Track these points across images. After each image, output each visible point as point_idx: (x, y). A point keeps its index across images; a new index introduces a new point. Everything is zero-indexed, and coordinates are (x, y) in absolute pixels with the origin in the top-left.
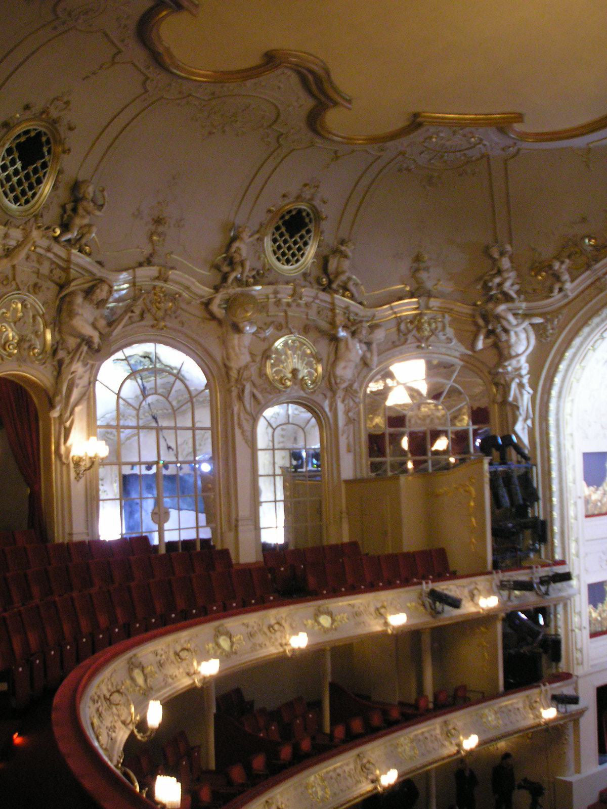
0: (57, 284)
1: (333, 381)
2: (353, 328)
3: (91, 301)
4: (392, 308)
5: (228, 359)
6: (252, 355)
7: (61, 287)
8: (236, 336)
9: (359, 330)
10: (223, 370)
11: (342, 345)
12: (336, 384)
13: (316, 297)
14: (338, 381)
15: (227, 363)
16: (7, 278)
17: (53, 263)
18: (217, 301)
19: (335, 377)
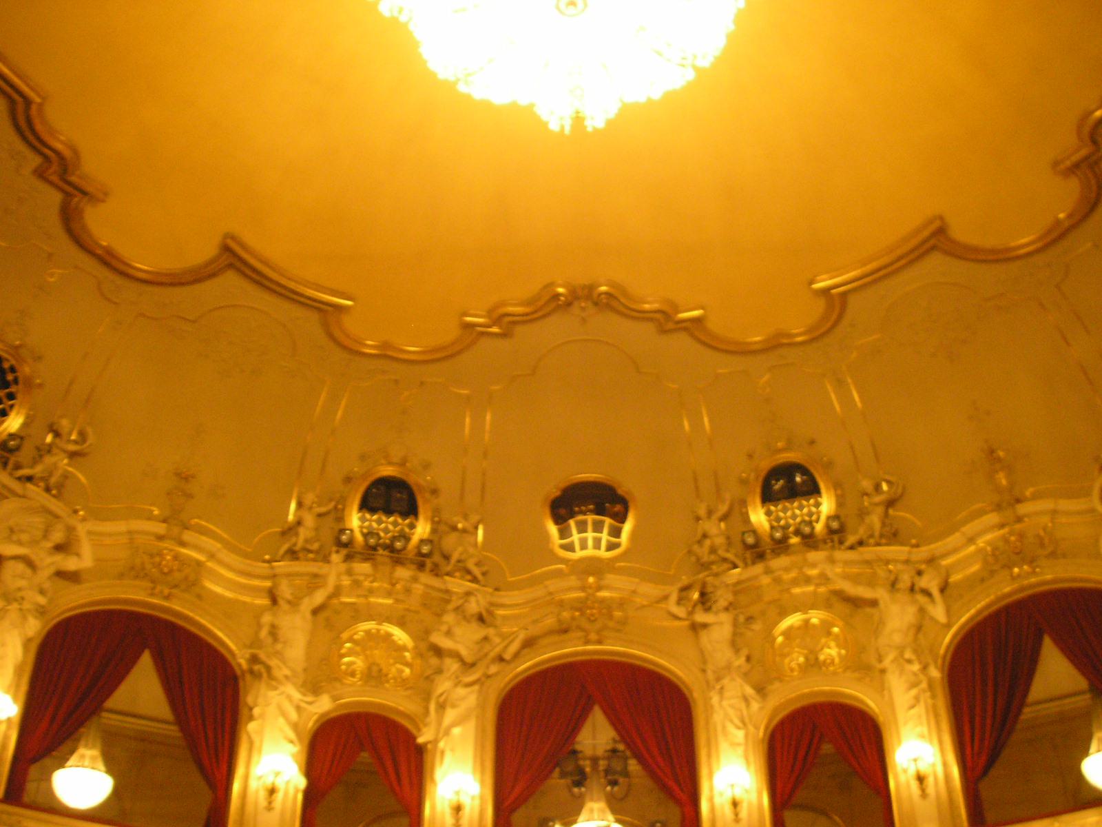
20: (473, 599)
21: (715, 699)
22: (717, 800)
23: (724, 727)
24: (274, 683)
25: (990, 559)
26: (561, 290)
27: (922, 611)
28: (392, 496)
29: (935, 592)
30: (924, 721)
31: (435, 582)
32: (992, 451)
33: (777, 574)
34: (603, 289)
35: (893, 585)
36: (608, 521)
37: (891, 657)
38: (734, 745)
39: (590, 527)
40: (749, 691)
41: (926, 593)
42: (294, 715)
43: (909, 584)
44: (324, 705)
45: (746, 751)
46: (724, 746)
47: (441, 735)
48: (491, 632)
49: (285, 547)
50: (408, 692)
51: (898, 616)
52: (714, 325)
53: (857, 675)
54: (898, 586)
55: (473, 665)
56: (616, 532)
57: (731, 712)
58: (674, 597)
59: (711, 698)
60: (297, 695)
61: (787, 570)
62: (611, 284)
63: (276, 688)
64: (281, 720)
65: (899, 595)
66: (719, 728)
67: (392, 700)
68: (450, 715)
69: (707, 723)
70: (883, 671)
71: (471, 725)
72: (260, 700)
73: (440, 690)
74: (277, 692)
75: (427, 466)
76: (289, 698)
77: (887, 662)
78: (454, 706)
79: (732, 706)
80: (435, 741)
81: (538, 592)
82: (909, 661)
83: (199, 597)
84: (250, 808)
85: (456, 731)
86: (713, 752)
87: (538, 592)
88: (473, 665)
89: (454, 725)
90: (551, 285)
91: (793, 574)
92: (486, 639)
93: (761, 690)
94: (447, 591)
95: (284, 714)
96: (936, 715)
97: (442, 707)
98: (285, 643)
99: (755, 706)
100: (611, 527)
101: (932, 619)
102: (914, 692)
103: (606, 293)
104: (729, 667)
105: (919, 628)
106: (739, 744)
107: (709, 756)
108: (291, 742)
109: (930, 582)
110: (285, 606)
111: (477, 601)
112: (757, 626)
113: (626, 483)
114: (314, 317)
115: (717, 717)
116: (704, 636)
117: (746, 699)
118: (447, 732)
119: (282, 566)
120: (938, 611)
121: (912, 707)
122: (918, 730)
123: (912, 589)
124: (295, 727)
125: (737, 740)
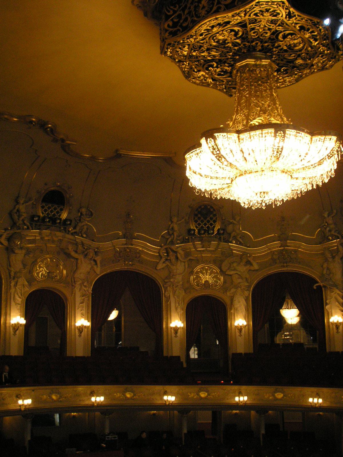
1: (73, 280)
2: (86, 253)
4: (112, 242)
5: (10, 266)
6: (25, 266)
8: (14, 255)
10: (7, 271)
11: (79, 261)
12: (75, 281)
14: (76, 281)
15: (9, 268)
18: (4, 236)
19: (74, 278)
21: (13, 284)
25: (118, 254)
27: (92, 267)
29: (98, 262)
30: (84, 308)
32: (128, 215)
33: (43, 236)
35: (86, 255)
37: (79, 283)
38: (16, 304)
40: (26, 283)
41: (95, 261)
45: (21, 307)
46: (13, 303)
51: (84, 267)
53: (64, 285)
58: (4, 236)
59: (10, 283)
61: (47, 236)
69: (7, 292)
82: (85, 286)
91: (49, 238)
93: (30, 284)
96: (88, 306)
99: (27, 289)
101: (95, 272)
102: (83, 298)
105: (89, 273)
109: (98, 259)
112: (31, 256)
115: (13, 290)
116: (13, 257)
120: (98, 270)
121: (81, 303)
123: (91, 259)
125: (18, 302)
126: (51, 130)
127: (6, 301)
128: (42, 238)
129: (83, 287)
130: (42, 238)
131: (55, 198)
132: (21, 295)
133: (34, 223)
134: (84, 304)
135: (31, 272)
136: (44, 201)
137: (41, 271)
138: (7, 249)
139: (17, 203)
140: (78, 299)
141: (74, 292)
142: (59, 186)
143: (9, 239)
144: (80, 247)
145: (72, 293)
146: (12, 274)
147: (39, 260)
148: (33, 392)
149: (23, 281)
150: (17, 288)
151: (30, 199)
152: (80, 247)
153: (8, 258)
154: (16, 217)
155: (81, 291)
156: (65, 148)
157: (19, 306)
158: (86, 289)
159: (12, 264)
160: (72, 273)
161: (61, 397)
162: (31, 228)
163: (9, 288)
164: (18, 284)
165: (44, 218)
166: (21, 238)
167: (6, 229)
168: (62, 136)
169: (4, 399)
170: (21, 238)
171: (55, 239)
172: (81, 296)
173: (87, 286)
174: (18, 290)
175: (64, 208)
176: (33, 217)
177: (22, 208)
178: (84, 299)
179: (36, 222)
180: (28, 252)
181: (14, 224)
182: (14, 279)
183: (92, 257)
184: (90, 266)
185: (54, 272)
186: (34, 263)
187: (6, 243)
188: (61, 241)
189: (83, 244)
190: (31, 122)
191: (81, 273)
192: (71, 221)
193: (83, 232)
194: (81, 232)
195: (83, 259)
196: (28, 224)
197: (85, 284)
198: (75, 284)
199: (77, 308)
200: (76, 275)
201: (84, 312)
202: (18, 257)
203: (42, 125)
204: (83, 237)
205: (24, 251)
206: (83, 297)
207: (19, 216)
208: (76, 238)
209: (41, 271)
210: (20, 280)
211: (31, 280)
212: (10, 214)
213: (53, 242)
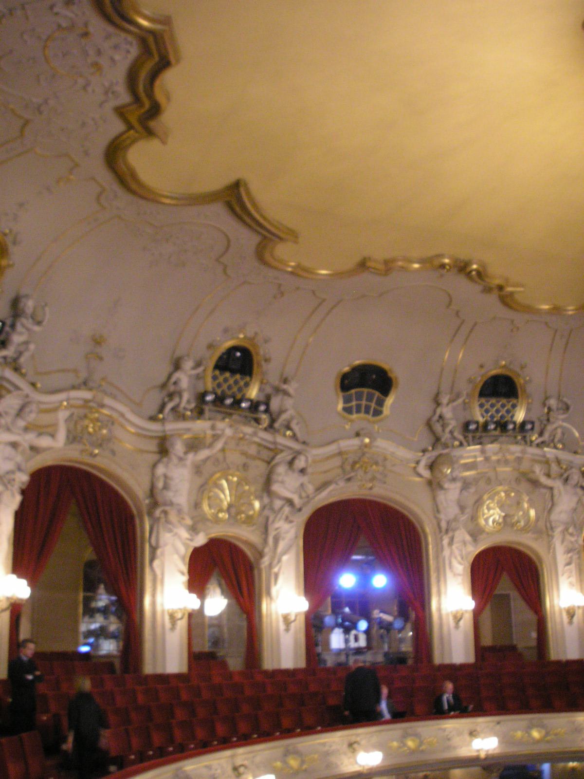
0: (263, 461)
1: (548, 525)
2: (565, 475)
3: (293, 471)
5: (438, 511)
6: (462, 508)
7: (269, 463)
8: (443, 492)
9: (570, 477)
10: (435, 521)
11: (556, 492)
13: (523, 452)
14: (553, 525)
15: (438, 515)
16: (217, 460)
17: (259, 445)
18: (423, 463)
19: (550, 522)
20: (302, 458)
21: (446, 541)
22: (444, 612)
23: (450, 563)
24: (170, 526)
26: (447, 261)
28: (238, 362)
30: (574, 572)
31: (268, 436)
33: (488, 455)
34: (475, 267)
36: (377, 394)
38: (455, 575)
39: (364, 399)
40: (468, 538)
42: (182, 550)
43: (576, 481)
44: (201, 540)
46: (449, 574)
47: (276, 561)
48: (305, 479)
49: (170, 406)
50: (254, 527)
52: (517, 297)
53: (533, 536)
54: (568, 482)
55: (300, 510)
56: (380, 403)
57: (457, 552)
58: (423, 463)
59: (442, 540)
60: (184, 534)
61: (496, 454)
62: (483, 265)
63: (170, 531)
64: (176, 557)
65: (568, 487)
66: (447, 562)
67: (244, 534)
68: (282, 545)
69: (437, 557)
70: (550, 537)
71: (293, 552)
72: (161, 542)
73: (277, 525)
74: (172, 534)
75: (266, 341)
76: (180, 537)
77: (557, 533)
78: (284, 539)
79: (457, 548)
80: (270, 566)
81: (332, 448)
82: (571, 535)
83: (113, 453)
84: (159, 630)
85: (285, 558)
86: (442, 579)
87: (332, 448)
88: (300, 510)
89: (285, 552)
90: (441, 256)
91: (499, 456)
92: (302, 485)
94: (275, 443)
95: (177, 551)
97: (276, 540)
98: (176, 491)
100: (378, 398)
102: (570, 555)
103: (475, 270)
104: (455, 519)
106: (459, 575)
107: (438, 581)
108: (183, 573)
110: (175, 460)
111: (307, 461)
112: (472, 490)
113: (397, 370)
114: (255, 239)
115: (446, 553)
116: (441, 496)
117: (464, 543)
118: (279, 561)
119: (171, 426)
121: (569, 564)
122: (570, 579)
123: (576, 486)
124: (183, 558)
126: (479, 273)
127: (438, 570)
128: (487, 459)
129: (568, 537)
130: (487, 459)
131: (501, 387)
132: (462, 558)
133: (470, 435)
134: (573, 566)
135: (474, 518)
136: (482, 394)
137: (492, 515)
138: (430, 483)
139: (438, 404)
140: (561, 558)
141: (552, 546)
142: (504, 367)
143: (431, 467)
144: (554, 468)
145: (549, 548)
146: (444, 525)
147: (485, 497)
148: (498, 727)
149: (462, 535)
150: (454, 547)
151: (458, 396)
152: (554, 468)
153: (434, 498)
154: (438, 428)
155: (565, 543)
156: (507, 300)
157: (460, 579)
158: (573, 539)
159: (441, 507)
160: (546, 513)
161: (547, 734)
162: (465, 443)
163: (439, 549)
164: (456, 540)
165: (486, 425)
166: (452, 462)
167: (424, 451)
168: (497, 282)
169: (449, 739)
170: (452, 462)
171: (509, 457)
172: (564, 553)
173: (575, 533)
174: (457, 552)
175: (518, 402)
176: (466, 425)
177: (447, 411)
178: (571, 558)
179: (473, 432)
180: (466, 485)
181: (437, 439)
182: (447, 531)
183: (578, 482)
184: (575, 499)
185: (513, 515)
186: (479, 503)
187: (426, 474)
188: (519, 460)
189: (558, 462)
190: (443, 266)
191: (561, 512)
192: (533, 423)
193: (556, 440)
194: (553, 441)
195: (562, 488)
196: (461, 437)
197: (571, 530)
198: (553, 532)
199: (560, 573)
200: (554, 516)
201: (573, 579)
202: (451, 495)
203: (462, 268)
204: (555, 447)
205: (459, 485)
206: (569, 551)
207: (444, 426)
208: (545, 452)
209: (492, 515)
210: (457, 533)
211: (476, 534)
212: (429, 424)
213: (506, 462)
